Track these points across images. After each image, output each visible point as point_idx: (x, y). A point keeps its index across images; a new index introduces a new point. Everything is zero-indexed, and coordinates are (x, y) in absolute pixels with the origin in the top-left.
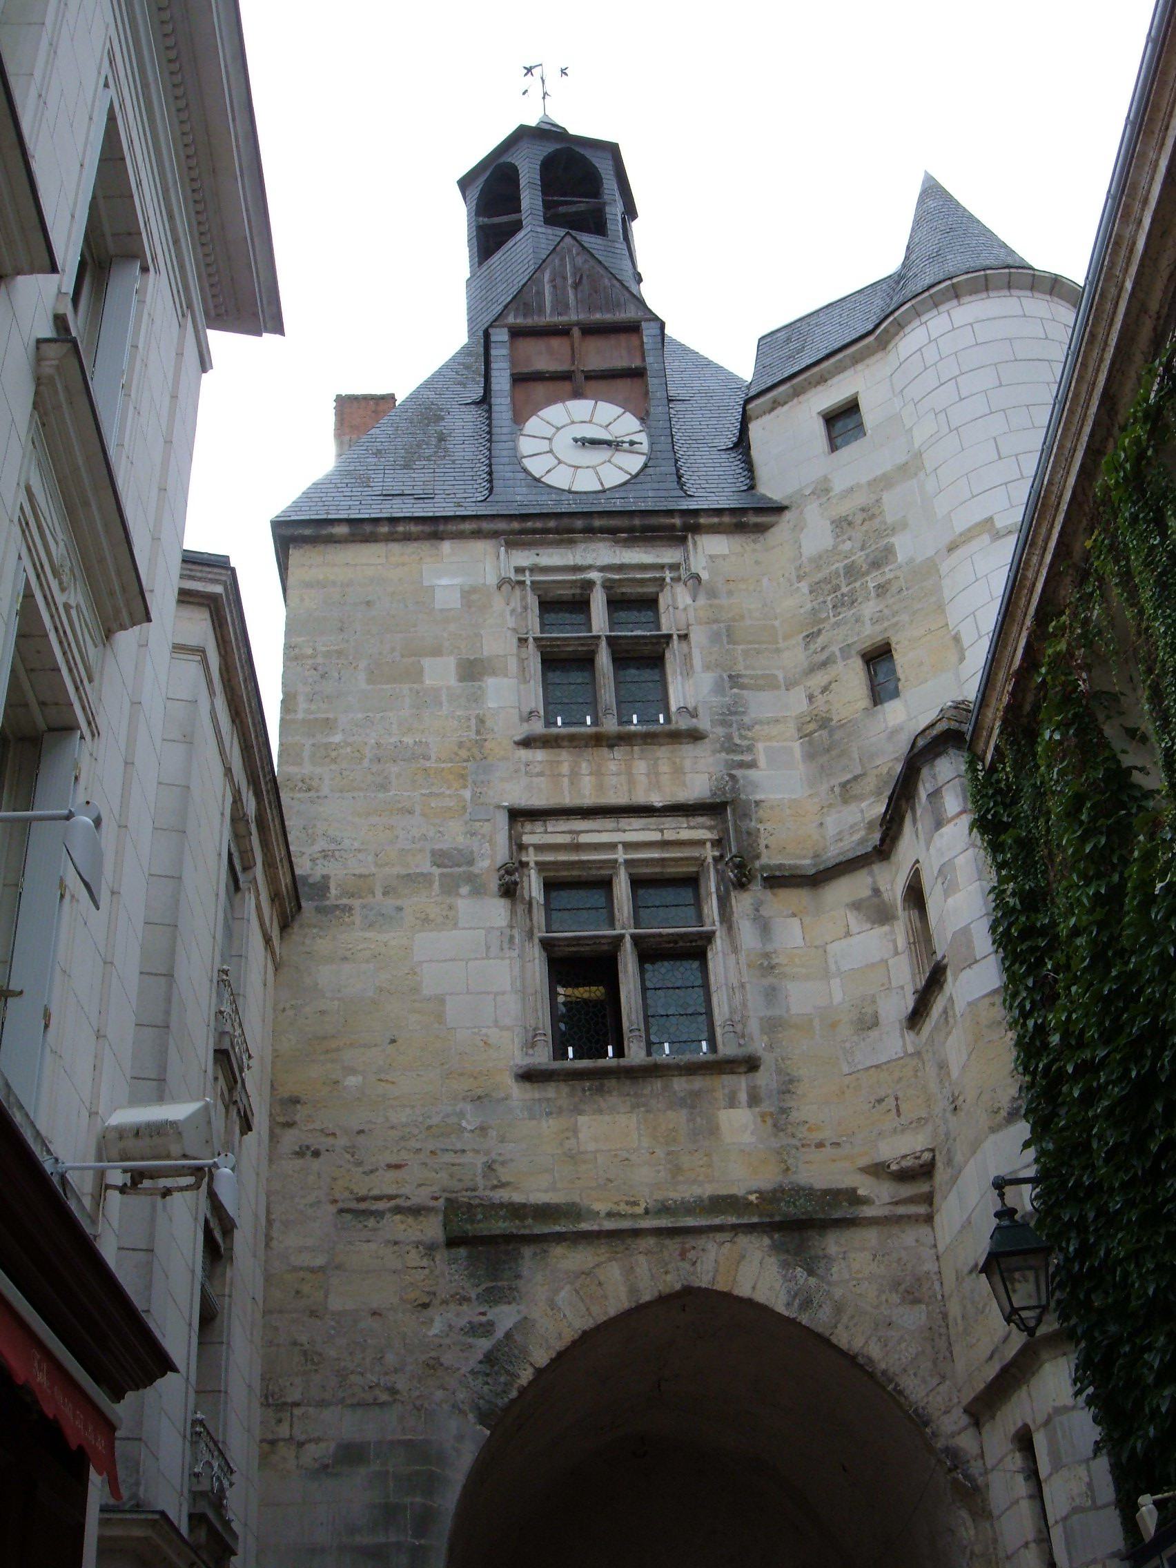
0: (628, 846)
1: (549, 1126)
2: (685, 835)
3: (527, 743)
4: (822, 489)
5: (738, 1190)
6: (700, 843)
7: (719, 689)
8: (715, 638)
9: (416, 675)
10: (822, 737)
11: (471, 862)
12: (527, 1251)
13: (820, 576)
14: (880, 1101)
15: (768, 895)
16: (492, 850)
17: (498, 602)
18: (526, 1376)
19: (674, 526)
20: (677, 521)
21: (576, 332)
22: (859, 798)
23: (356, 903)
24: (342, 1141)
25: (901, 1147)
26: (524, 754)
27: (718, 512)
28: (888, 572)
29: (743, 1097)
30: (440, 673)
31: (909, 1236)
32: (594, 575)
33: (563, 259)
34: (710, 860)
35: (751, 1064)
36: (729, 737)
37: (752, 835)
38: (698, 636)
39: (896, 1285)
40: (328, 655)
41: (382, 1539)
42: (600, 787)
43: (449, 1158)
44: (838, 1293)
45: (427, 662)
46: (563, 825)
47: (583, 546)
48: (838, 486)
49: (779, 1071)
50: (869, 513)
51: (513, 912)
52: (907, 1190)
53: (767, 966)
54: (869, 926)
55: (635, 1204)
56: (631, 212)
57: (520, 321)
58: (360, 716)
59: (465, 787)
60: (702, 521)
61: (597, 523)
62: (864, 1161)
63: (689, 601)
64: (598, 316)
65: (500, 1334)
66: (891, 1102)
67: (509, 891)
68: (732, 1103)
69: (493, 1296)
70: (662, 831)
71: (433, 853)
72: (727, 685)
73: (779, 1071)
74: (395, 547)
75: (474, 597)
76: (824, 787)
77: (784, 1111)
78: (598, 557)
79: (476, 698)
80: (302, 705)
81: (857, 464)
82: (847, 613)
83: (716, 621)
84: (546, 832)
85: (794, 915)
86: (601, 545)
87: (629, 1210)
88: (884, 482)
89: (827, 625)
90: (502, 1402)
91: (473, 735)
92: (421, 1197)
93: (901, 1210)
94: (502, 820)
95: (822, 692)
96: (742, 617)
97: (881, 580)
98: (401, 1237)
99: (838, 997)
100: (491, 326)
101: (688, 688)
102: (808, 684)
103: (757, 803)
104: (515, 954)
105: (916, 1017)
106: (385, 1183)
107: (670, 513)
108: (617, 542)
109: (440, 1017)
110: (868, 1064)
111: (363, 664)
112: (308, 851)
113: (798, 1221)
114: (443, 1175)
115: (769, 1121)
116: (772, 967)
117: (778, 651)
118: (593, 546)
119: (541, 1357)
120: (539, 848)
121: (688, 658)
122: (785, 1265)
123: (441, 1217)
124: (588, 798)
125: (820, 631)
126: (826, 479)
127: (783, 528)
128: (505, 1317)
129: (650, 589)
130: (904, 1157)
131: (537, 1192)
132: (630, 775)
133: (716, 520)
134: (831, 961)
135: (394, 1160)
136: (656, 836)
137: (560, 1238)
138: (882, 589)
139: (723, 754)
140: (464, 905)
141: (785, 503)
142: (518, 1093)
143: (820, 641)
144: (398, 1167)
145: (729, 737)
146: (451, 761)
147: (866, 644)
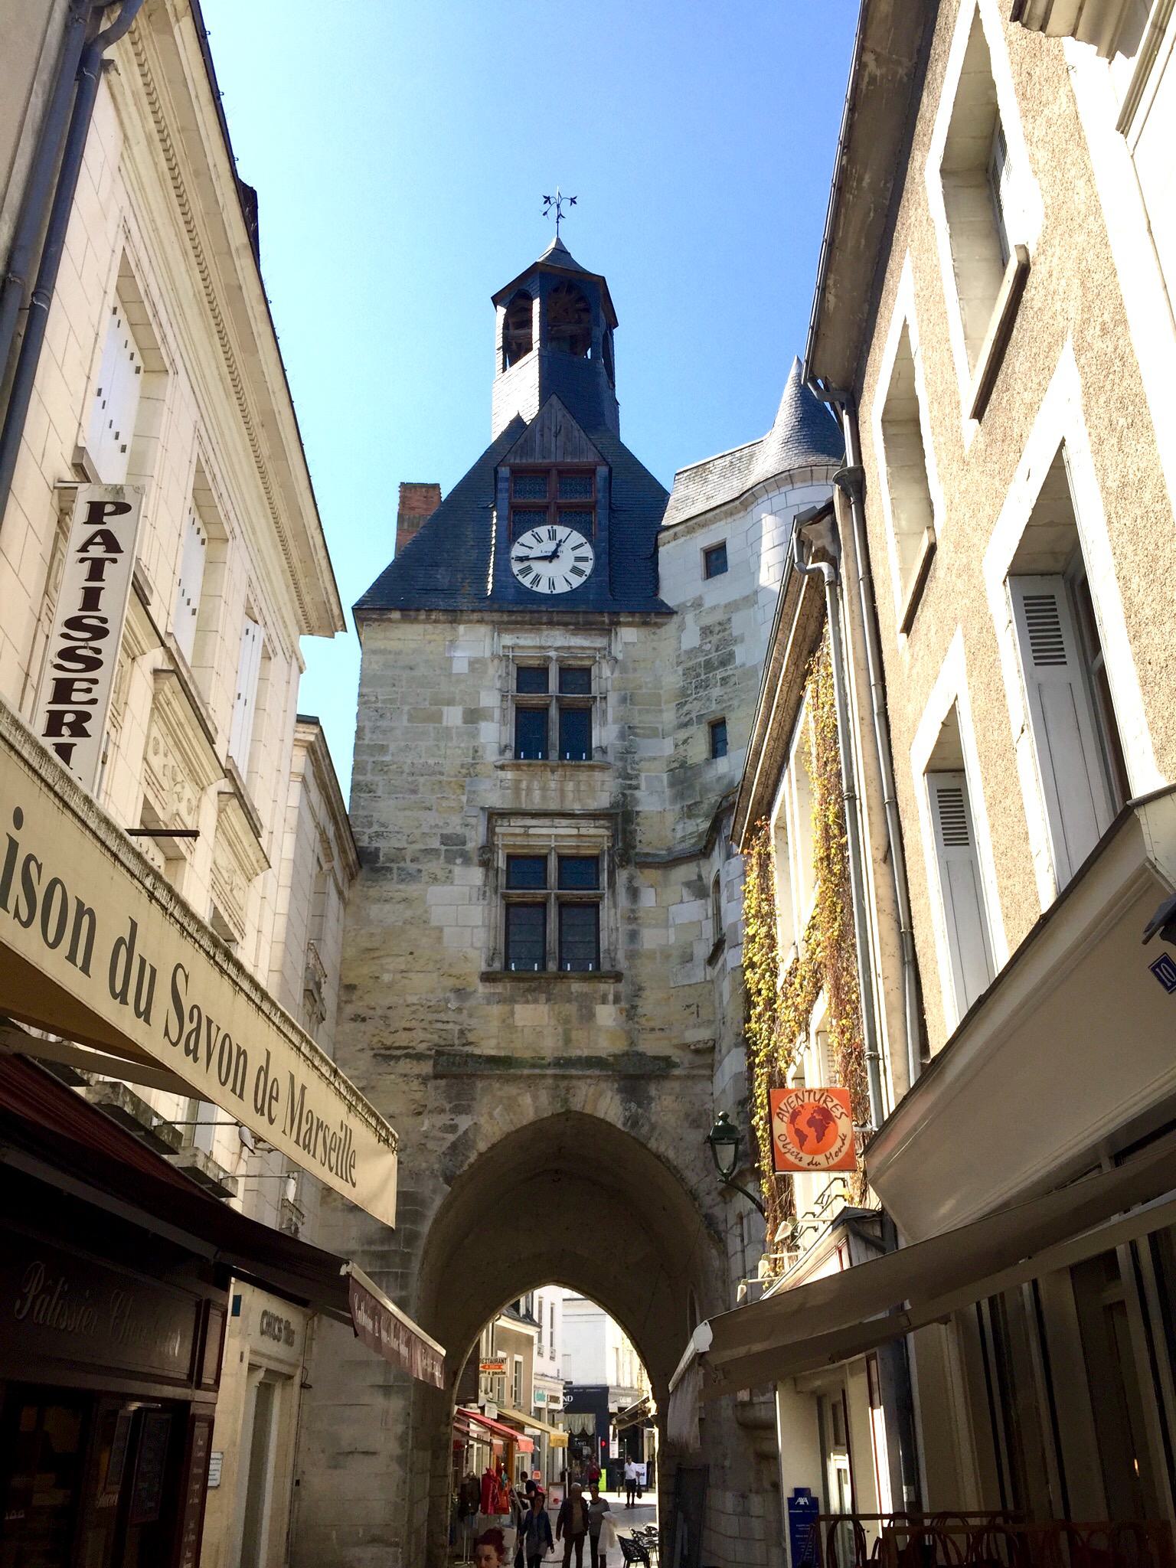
1: (496, 1010)
2: (592, 831)
3: (502, 768)
4: (698, 604)
7: (622, 736)
8: (623, 700)
9: (437, 718)
10: (683, 777)
11: (464, 843)
12: (480, 1085)
13: (690, 664)
16: (476, 838)
18: (473, 1157)
21: (554, 472)
22: (698, 816)
23: (394, 866)
24: (379, 1012)
25: (699, 1035)
26: (501, 774)
28: (729, 671)
29: (611, 997)
30: (453, 716)
31: (699, 1087)
32: (552, 654)
35: (618, 977)
36: (625, 768)
37: (633, 832)
38: (613, 699)
39: (687, 1115)
40: (384, 701)
41: (386, 1248)
42: (544, 798)
43: (439, 1026)
45: (445, 709)
46: (520, 822)
47: (545, 633)
48: (708, 603)
49: (633, 984)
50: (724, 625)
51: (487, 876)
52: (699, 1060)
53: (632, 918)
56: (614, 323)
58: (403, 744)
62: (675, 1041)
65: (460, 1132)
66: (694, 1008)
67: (486, 864)
68: (604, 1001)
69: (458, 1110)
73: (633, 984)
74: (429, 627)
76: (678, 806)
77: (634, 1007)
78: (555, 643)
79: (474, 735)
80: (368, 735)
81: (720, 591)
82: (702, 693)
86: (557, 633)
88: (733, 607)
89: (690, 699)
92: (422, 1048)
93: (695, 1072)
97: (725, 674)
98: (408, 1071)
99: (672, 940)
101: (603, 734)
103: (638, 813)
105: (712, 960)
106: (402, 1039)
109: (439, 939)
111: (406, 708)
112: (368, 831)
113: (636, 1074)
114: (435, 1037)
117: (661, 711)
118: (553, 633)
119: (482, 1146)
121: (604, 712)
123: (431, 1062)
124: (536, 802)
126: (701, 598)
128: (464, 1122)
129: (587, 663)
131: (489, 1048)
132: (562, 791)
135: (408, 1025)
136: (574, 832)
138: (724, 681)
140: (458, 870)
142: (482, 989)
143: (686, 708)
144: (410, 1029)
145: (625, 768)
147: (711, 717)
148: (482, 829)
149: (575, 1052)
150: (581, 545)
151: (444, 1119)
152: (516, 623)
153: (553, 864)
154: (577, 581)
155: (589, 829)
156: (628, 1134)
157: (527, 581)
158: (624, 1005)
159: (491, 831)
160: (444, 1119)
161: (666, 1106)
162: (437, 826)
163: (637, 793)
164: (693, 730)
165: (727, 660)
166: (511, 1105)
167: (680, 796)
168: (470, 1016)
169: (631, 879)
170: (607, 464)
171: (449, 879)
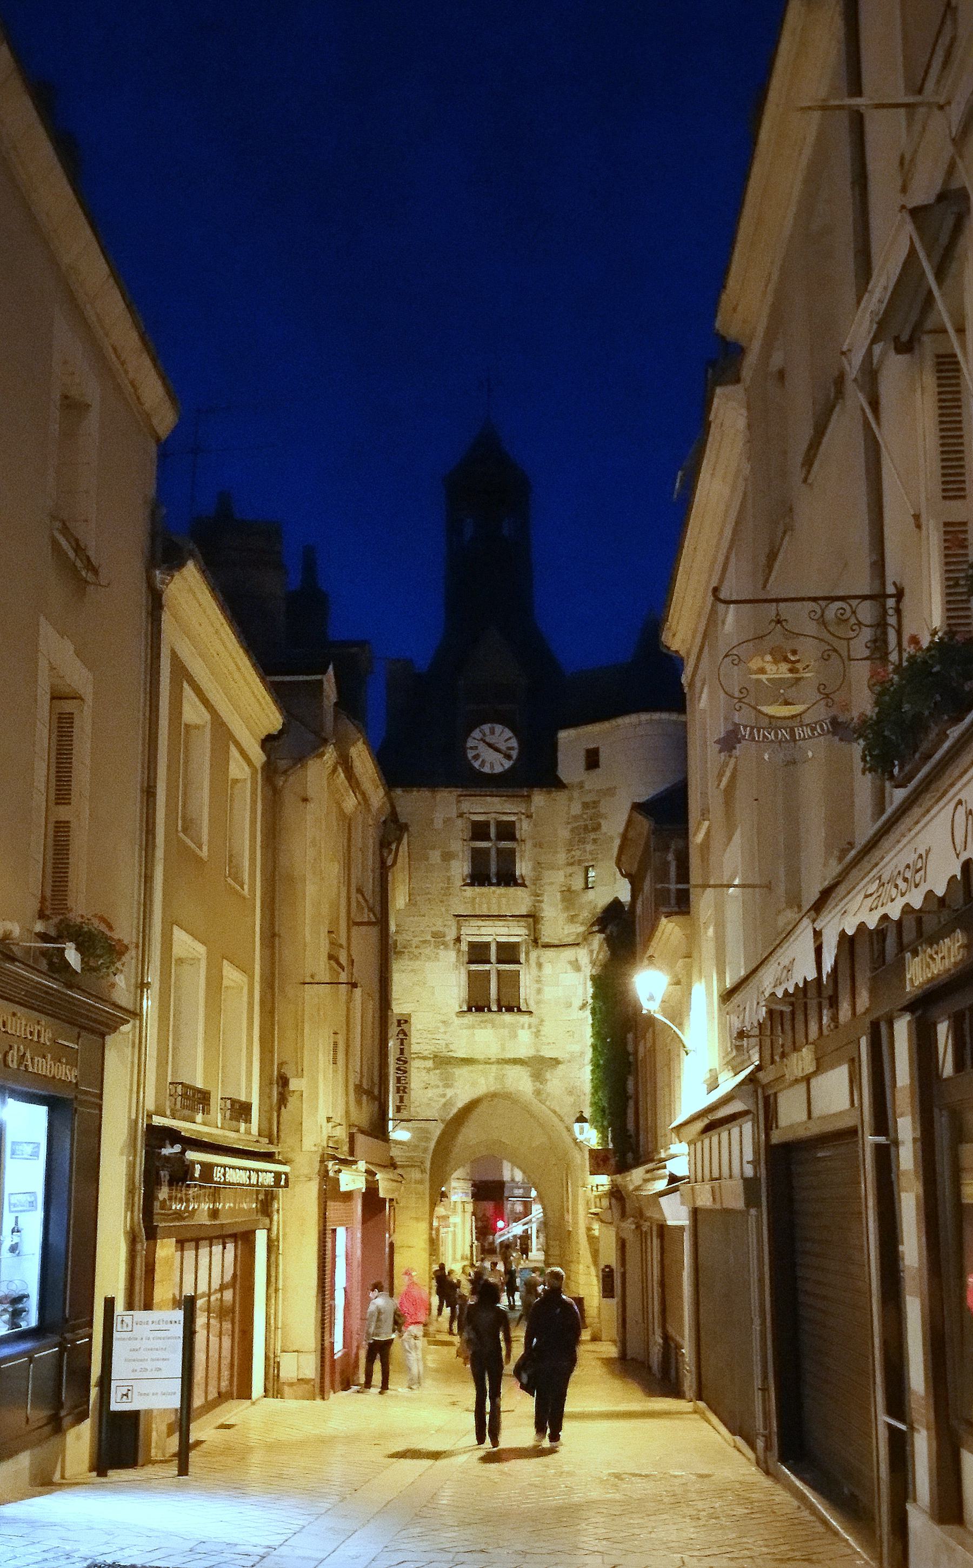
7: (534, 869)
29: (526, 1026)
37: (540, 930)
42: (489, 910)
43: (434, 1041)
48: (587, 786)
50: (595, 804)
68: (523, 1028)
69: (447, 1086)
76: (566, 915)
92: (426, 1053)
122: (534, 1081)
128: (450, 1093)
138: (595, 841)
142: (457, 1021)
148: (454, 928)
151: (440, 1091)
158: (534, 1030)
160: (440, 1091)
165: (597, 828)
166: (474, 1084)
169: (538, 957)
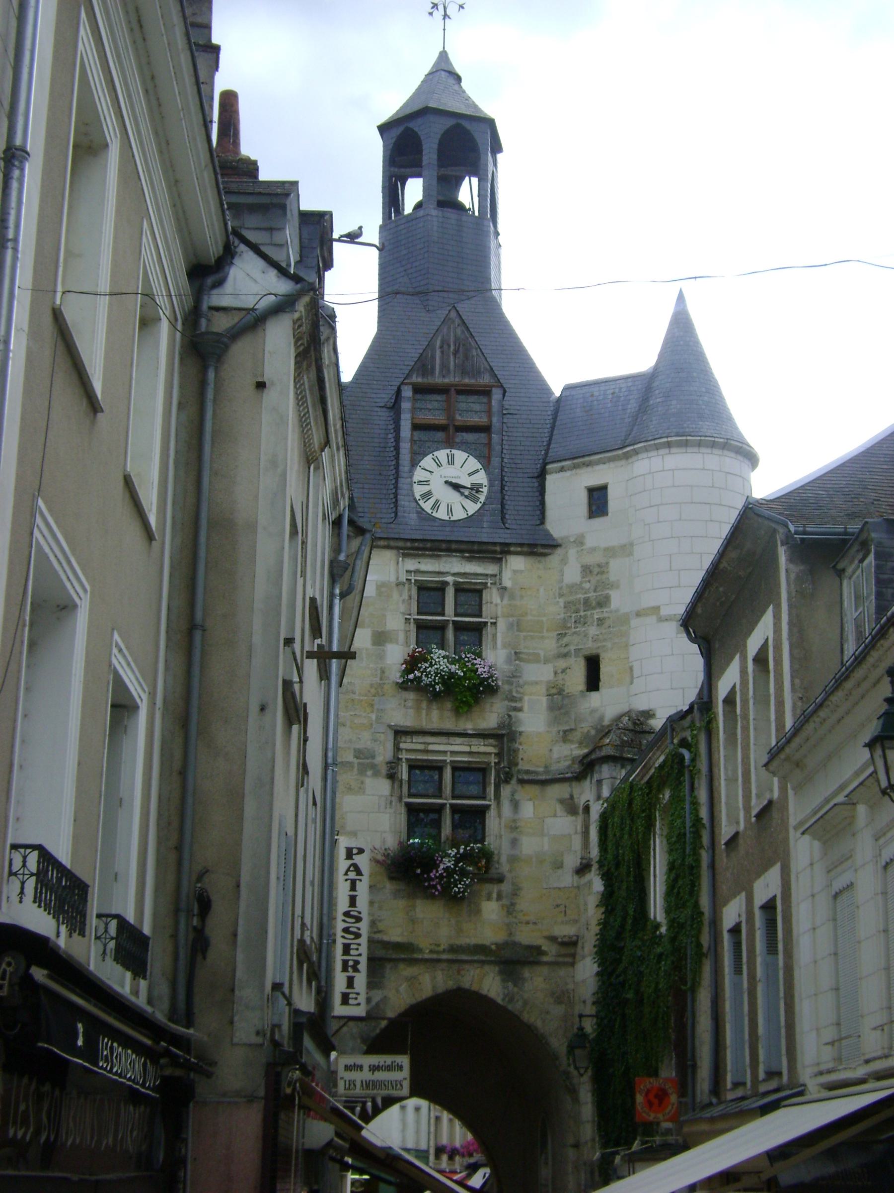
0: (452, 753)
2: (482, 749)
5: (487, 943)
6: (490, 754)
7: (509, 661)
8: (510, 626)
10: (559, 701)
11: (373, 757)
12: (388, 966)
13: (571, 598)
14: (558, 906)
15: (519, 788)
16: (384, 753)
17: (395, 595)
19: (495, 553)
20: (498, 548)
21: (453, 392)
27: (521, 545)
29: (495, 895)
31: (562, 972)
32: (450, 579)
33: (449, 328)
34: (493, 764)
36: (510, 691)
37: (516, 751)
38: (502, 625)
39: (552, 994)
44: (526, 996)
46: (421, 739)
47: (444, 559)
49: (513, 884)
51: (393, 787)
52: (564, 950)
53: (514, 827)
54: (565, 814)
55: (439, 945)
57: (420, 380)
59: (372, 712)
60: (512, 549)
61: (454, 546)
62: (546, 934)
63: (499, 601)
64: (467, 381)
67: (392, 777)
68: (489, 898)
70: (470, 746)
71: (355, 750)
72: (513, 657)
73: (513, 884)
75: (383, 589)
76: (556, 729)
77: (513, 904)
78: (453, 568)
79: (381, 657)
83: (512, 616)
84: (412, 742)
85: (530, 800)
86: (454, 559)
87: (437, 949)
90: (373, 1034)
91: (378, 680)
93: (561, 959)
94: (391, 735)
95: (562, 672)
96: (526, 614)
99: (546, 847)
100: (402, 383)
102: (557, 664)
104: (392, 811)
107: (494, 544)
108: (463, 557)
110: (556, 885)
113: (513, 960)
115: (505, 909)
116: (517, 828)
117: (543, 638)
118: (450, 559)
120: (408, 751)
122: (503, 981)
125: (566, 634)
127: (554, 559)
130: (565, 936)
133: (519, 549)
134: (545, 827)
136: (467, 749)
137: (404, 960)
139: (506, 702)
141: (560, 542)
146: (366, 695)
148: (390, 745)
149: (463, 941)
150: (477, 471)
152: (418, 549)
153: (448, 774)
154: (473, 508)
155: (480, 746)
156: (504, 1009)
157: (427, 506)
159: (397, 749)
161: (536, 984)
162: (350, 741)
163: (520, 714)
164: (571, 661)
167: (555, 721)
168: (380, 908)
170: (502, 386)
171: (361, 790)
